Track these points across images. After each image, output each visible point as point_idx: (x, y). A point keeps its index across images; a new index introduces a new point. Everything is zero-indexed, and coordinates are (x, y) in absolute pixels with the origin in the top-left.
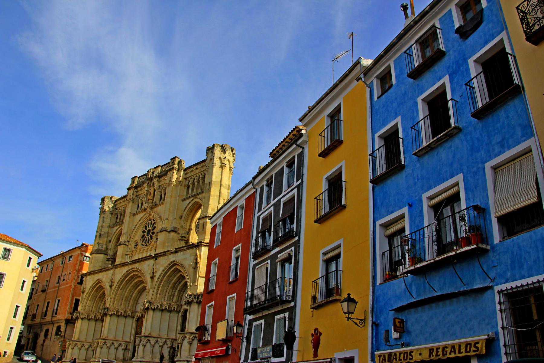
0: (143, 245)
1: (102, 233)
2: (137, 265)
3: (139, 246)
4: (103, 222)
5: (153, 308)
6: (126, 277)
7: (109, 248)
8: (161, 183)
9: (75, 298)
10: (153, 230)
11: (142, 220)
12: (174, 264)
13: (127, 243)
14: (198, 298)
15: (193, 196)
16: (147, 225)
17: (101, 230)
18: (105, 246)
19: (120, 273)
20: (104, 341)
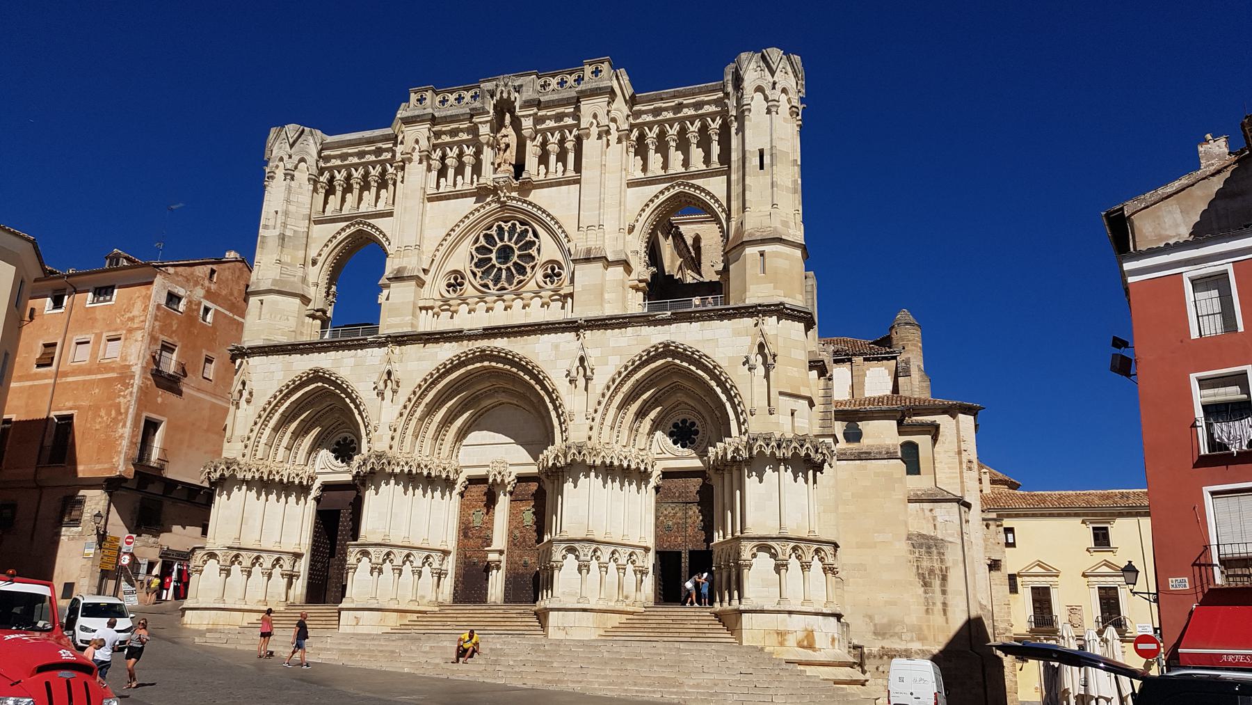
0: (486, 286)
1: (288, 233)
2: (500, 343)
4: (288, 201)
5: (598, 462)
6: (448, 372)
7: (312, 279)
9: (144, 415)
10: (519, 249)
12: (667, 350)
13: (422, 275)
16: (493, 232)
17: (285, 225)
18: (300, 273)
19: (419, 359)
20: (386, 550)
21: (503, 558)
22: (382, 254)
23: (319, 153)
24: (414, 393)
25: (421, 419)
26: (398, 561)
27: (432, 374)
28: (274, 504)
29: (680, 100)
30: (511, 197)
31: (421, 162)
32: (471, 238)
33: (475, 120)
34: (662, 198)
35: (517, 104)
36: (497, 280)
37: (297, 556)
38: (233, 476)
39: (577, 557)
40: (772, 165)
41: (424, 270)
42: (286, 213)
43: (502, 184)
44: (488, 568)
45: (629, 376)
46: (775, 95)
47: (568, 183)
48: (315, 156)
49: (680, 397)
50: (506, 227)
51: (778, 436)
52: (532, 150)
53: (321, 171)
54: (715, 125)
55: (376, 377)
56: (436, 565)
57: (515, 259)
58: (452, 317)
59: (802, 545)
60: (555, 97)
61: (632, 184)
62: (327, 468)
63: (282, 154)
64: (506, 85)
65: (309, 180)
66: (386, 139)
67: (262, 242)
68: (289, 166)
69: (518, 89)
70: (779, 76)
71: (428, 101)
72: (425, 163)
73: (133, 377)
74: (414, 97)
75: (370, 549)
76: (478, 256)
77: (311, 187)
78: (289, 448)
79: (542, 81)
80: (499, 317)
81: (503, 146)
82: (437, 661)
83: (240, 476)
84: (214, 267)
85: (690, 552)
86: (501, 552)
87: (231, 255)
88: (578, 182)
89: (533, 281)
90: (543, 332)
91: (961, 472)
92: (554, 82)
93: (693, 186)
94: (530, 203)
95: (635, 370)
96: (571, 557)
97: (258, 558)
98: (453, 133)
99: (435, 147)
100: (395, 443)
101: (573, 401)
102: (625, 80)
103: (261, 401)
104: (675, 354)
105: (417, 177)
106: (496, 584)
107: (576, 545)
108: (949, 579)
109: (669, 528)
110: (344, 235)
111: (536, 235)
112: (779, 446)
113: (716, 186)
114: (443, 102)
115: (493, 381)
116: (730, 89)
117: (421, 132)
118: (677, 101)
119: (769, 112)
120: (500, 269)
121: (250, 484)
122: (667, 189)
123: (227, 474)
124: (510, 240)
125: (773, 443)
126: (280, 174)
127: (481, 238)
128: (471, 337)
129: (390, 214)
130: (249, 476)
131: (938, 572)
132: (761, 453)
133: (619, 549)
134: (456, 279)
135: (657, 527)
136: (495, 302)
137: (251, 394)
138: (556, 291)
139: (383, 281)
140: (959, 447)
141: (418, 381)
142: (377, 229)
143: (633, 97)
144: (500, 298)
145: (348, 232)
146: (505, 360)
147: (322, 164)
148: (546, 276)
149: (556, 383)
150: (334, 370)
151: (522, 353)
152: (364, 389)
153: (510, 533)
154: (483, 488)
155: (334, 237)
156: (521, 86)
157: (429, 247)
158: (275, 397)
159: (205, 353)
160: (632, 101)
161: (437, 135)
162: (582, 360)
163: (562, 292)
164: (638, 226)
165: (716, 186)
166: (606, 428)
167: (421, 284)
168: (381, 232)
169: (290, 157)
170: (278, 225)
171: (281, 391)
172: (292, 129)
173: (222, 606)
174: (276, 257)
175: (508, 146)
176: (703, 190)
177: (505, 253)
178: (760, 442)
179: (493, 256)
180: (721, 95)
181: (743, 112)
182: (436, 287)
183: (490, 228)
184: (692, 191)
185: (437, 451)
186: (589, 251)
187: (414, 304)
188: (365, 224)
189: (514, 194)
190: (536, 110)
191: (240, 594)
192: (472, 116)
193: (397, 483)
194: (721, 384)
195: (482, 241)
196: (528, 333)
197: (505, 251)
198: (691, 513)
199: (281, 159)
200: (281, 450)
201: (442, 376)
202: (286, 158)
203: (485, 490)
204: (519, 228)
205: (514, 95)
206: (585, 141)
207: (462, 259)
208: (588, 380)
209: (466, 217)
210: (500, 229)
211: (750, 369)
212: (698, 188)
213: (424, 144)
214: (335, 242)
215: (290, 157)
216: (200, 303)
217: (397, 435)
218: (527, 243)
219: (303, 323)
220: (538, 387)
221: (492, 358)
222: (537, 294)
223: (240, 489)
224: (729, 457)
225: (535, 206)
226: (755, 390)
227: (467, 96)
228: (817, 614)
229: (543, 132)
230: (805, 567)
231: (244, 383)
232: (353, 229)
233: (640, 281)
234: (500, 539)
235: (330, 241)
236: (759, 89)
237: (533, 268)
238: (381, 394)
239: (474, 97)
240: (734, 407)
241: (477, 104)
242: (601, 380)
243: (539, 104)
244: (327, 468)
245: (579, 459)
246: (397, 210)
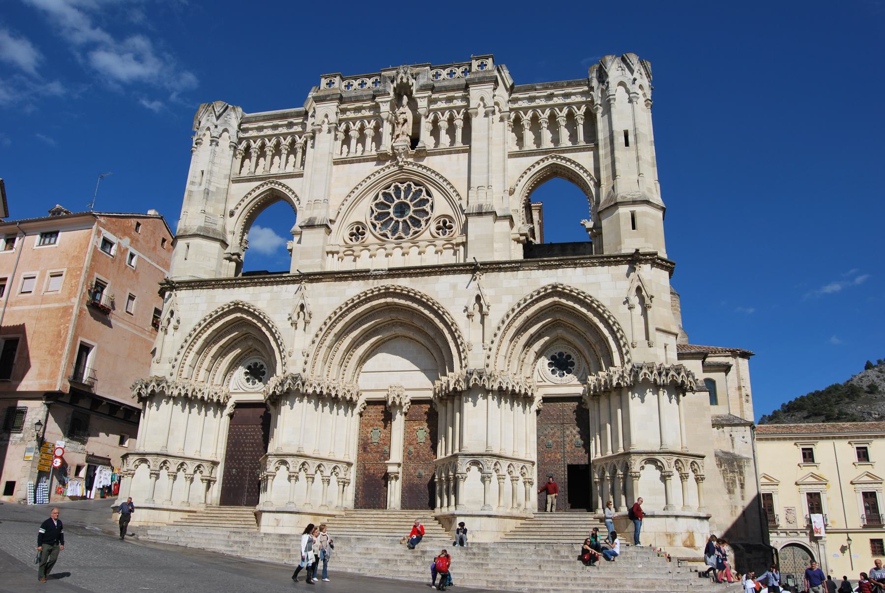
0: (385, 235)
1: (212, 189)
2: (403, 282)
4: (212, 162)
5: (496, 387)
6: (355, 306)
7: (229, 228)
9: (80, 339)
12: (555, 291)
13: (329, 224)
14: (667, 374)
15: (546, 152)
16: (391, 191)
18: (220, 222)
20: (302, 460)
21: (400, 470)
22: (292, 210)
23: (239, 126)
24: (325, 324)
25: (330, 347)
26: (311, 470)
27: (341, 308)
28: (196, 416)
29: (552, 91)
30: (408, 163)
31: (329, 131)
32: (372, 195)
33: (378, 100)
34: (538, 168)
35: (414, 89)
36: (394, 231)
37: (215, 464)
38: (162, 392)
39: (480, 470)
40: (636, 142)
41: (331, 221)
42: (211, 173)
43: (400, 151)
44: (387, 477)
45: (521, 312)
46: (635, 88)
47: (458, 152)
48: (236, 128)
49: (560, 332)
50: (403, 187)
51: (658, 364)
52: (426, 126)
53: (240, 140)
54: (580, 113)
55: (291, 309)
56: (341, 475)
57: (411, 213)
58: (355, 260)
59: (682, 459)
60: (446, 83)
61: (512, 155)
62: (241, 388)
63: (209, 124)
64: (405, 73)
65: (230, 146)
66: (298, 115)
67: (190, 196)
68: (215, 135)
69: (415, 76)
70: (636, 75)
71: (336, 85)
72: (333, 133)
73: (72, 307)
74: (324, 82)
75: (288, 459)
76: (377, 211)
77: (232, 153)
78: (209, 370)
79: (434, 72)
80: (398, 261)
81: (401, 121)
82: (376, 562)
83: (168, 392)
84: (139, 221)
85: (569, 466)
86: (399, 465)
87: (151, 212)
88: (469, 151)
89: (427, 232)
90: (442, 273)
91: (741, 404)
92: (444, 73)
93: (564, 159)
94: (425, 168)
95: (526, 308)
96: (474, 469)
97: (182, 464)
98: (358, 110)
99: (341, 121)
100: (308, 367)
101: (470, 332)
102: (506, 73)
103: (187, 328)
104: (562, 294)
105: (326, 145)
106: (395, 492)
107: (479, 459)
108: (746, 487)
109: (549, 446)
110: (258, 192)
111: (429, 194)
112: (660, 374)
113: (585, 159)
114: (348, 86)
115: (393, 315)
116: (595, 83)
117: (330, 109)
118: (549, 92)
119: (630, 101)
120: (397, 222)
121: (176, 399)
122: (543, 160)
123: (157, 390)
124: (406, 198)
125: (655, 372)
126: (206, 140)
127: (380, 196)
128: (375, 277)
129: (301, 175)
130: (176, 393)
131: (737, 482)
132: (645, 380)
133: (514, 463)
134: (358, 229)
135: (538, 445)
136: (394, 248)
137: (178, 321)
139: (296, 228)
140: (739, 383)
141: (329, 313)
142: (287, 188)
143: (512, 87)
144: (399, 246)
145: (262, 189)
146: (407, 297)
147: (241, 135)
148: (438, 228)
149: (455, 317)
150: (252, 303)
151: (423, 292)
152: (279, 320)
153: (405, 449)
154: (381, 408)
155: (250, 194)
156: (418, 74)
157: (335, 203)
158: (200, 325)
159: (129, 291)
160: (511, 90)
161: (343, 111)
162: (478, 298)
163: (454, 242)
164: (518, 190)
165: (585, 159)
166: (501, 359)
167: (329, 231)
168: (291, 190)
169: (216, 127)
170: (204, 182)
171: (205, 320)
172: (219, 107)
173: (152, 506)
174: (201, 208)
175: (405, 121)
176: (574, 162)
177: (402, 209)
178: (645, 370)
179: (391, 210)
180: (586, 88)
181: (609, 100)
182: (340, 235)
183: (389, 187)
184: (563, 163)
185: (341, 376)
186: (481, 206)
187: (323, 248)
188: (277, 183)
189: (410, 160)
190: (430, 93)
191: (166, 496)
192: (374, 97)
193: (309, 402)
194: (605, 322)
195: (381, 199)
196: (429, 274)
197: (401, 207)
198: (568, 432)
199: (208, 129)
200: (203, 372)
201: (350, 310)
202: (212, 128)
203: (385, 410)
205: (412, 81)
206: (473, 119)
207: (363, 212)
208: (483, 316)
209: (368, 178)
210: (397, 188)
211: (630, 308)
212: (569, 160)
213: (333, 118)
214: (250, 198)
215: (216, 127)
216: (127, 249)
217: (310, 360)
218: (421, 200)
219: (221, 265)
220: (437, 321)
221: (395, 294)
222: (432, 243)
223: (167, 403)
224: (614, 383)
225: (430, 169)
226: (636, 326)
227: (369, 82)
228: (696, 517)
229: (435, 111)
230: (683, 477)
231: (172, 313)
232: (266, 188)
233: (521, 235)
234: (397, 454)
235: (246, 197)
236: (621, 84)
237: (427, 221)
238: (294, 324)
239: (375, 83)
240: (617, 340)
241: (379, 87)
242: (494, 318)
243: (433, 89)
244: (241, 388)
245: (480, 383)
246: (307, 171)
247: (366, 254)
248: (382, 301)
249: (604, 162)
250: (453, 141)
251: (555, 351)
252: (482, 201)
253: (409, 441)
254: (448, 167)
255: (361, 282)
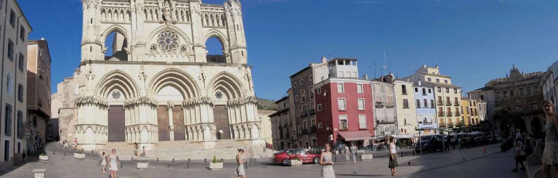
2: (177, 67)
3: (158, 49)
8: (177, 6)
11: (159, 29)
16: (164, 34)
36: (167, 48)
42: (95, 19)
49: (220, 85)
50: (168, 33)
101: (200, 84)
110: (111, 28)
111: (177, 36)
128: (168, 64)
138: (186, 53)
141: (153, 75)
145: (113, 27)
160: (201, 5)
162: (202, 74)
165: (224, 31)
177: (168, 41)
195: (160, 37)
203: (166, 108)
204: (172, 34)
214: (108, 30)
222: (180, 54)
232: (114, 27)
247: (158, 55)
248: (170, 73)
249: (232, 34)
250: (183, 20)
251: (217, 91)
252: (198, 42)
253: (174, 119)
254: (183, 28)
255: (163, 66)
